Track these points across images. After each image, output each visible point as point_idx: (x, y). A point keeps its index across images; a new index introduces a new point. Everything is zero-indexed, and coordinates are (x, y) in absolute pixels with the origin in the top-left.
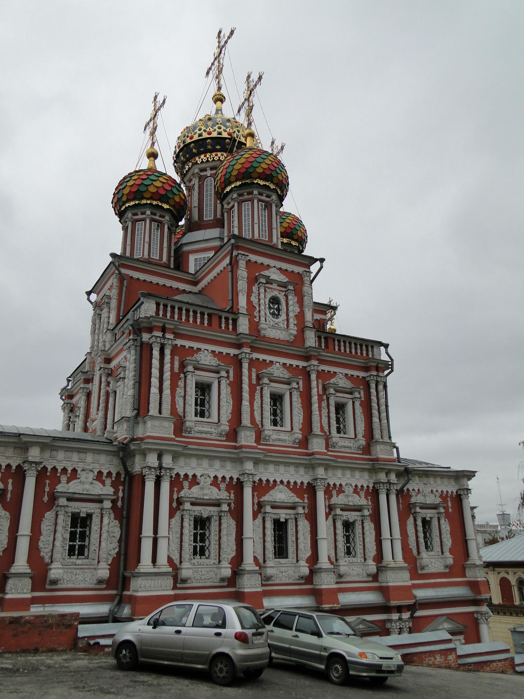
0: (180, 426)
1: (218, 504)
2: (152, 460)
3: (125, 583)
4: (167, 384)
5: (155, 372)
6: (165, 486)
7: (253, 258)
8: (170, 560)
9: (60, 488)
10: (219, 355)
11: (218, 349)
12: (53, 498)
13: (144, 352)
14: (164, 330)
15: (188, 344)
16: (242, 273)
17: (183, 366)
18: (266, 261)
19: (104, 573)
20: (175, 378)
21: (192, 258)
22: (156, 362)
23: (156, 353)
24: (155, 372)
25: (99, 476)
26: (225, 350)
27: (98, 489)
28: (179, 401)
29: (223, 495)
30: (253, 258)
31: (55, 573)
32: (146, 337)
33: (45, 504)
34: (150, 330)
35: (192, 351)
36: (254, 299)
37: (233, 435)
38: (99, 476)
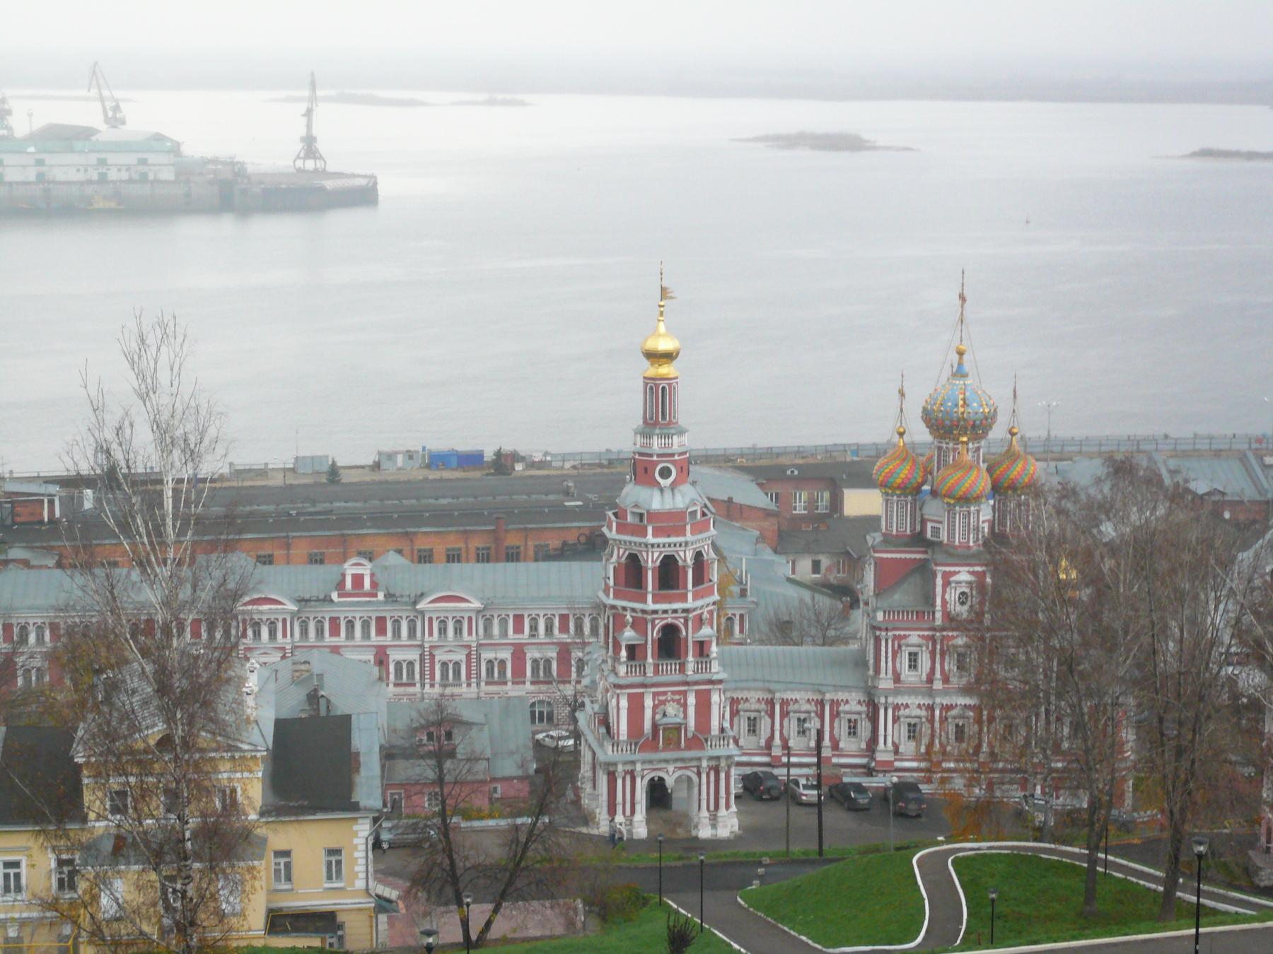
0: (897, 678)
1: (920, 717)
2: (882, 700)
3: (874, 751)
4: (890, 659)
5: (883, 654)
6: (890, 712)
7: (948, 569)
8: (894, 743)
9: (841, 708)
10: (922, 637)
11: (921, 633)
12: (838, 714)
13: (877, 640)
14: (887, 629)
15: (902, 633)
16: (939, 581)
17: (900, 646)
18: (957, 569)
19: (863, 746)
20: (895, 654)
21: (929, 525)
22: (883, 649)
23: (883, 643)
24: (883, 654)
25: (859, 702)
26: (926, 633)
27: (859, 708)
28: (898, 665)
29: (923, 713)
30: (948, 569)
31: (841, 745)
32: (878, 633)
33: (835, 715)
34: (880, 629)
35: (905, 637)
36: (947, 597)
37: (930, 680)
38: (859, 702)
